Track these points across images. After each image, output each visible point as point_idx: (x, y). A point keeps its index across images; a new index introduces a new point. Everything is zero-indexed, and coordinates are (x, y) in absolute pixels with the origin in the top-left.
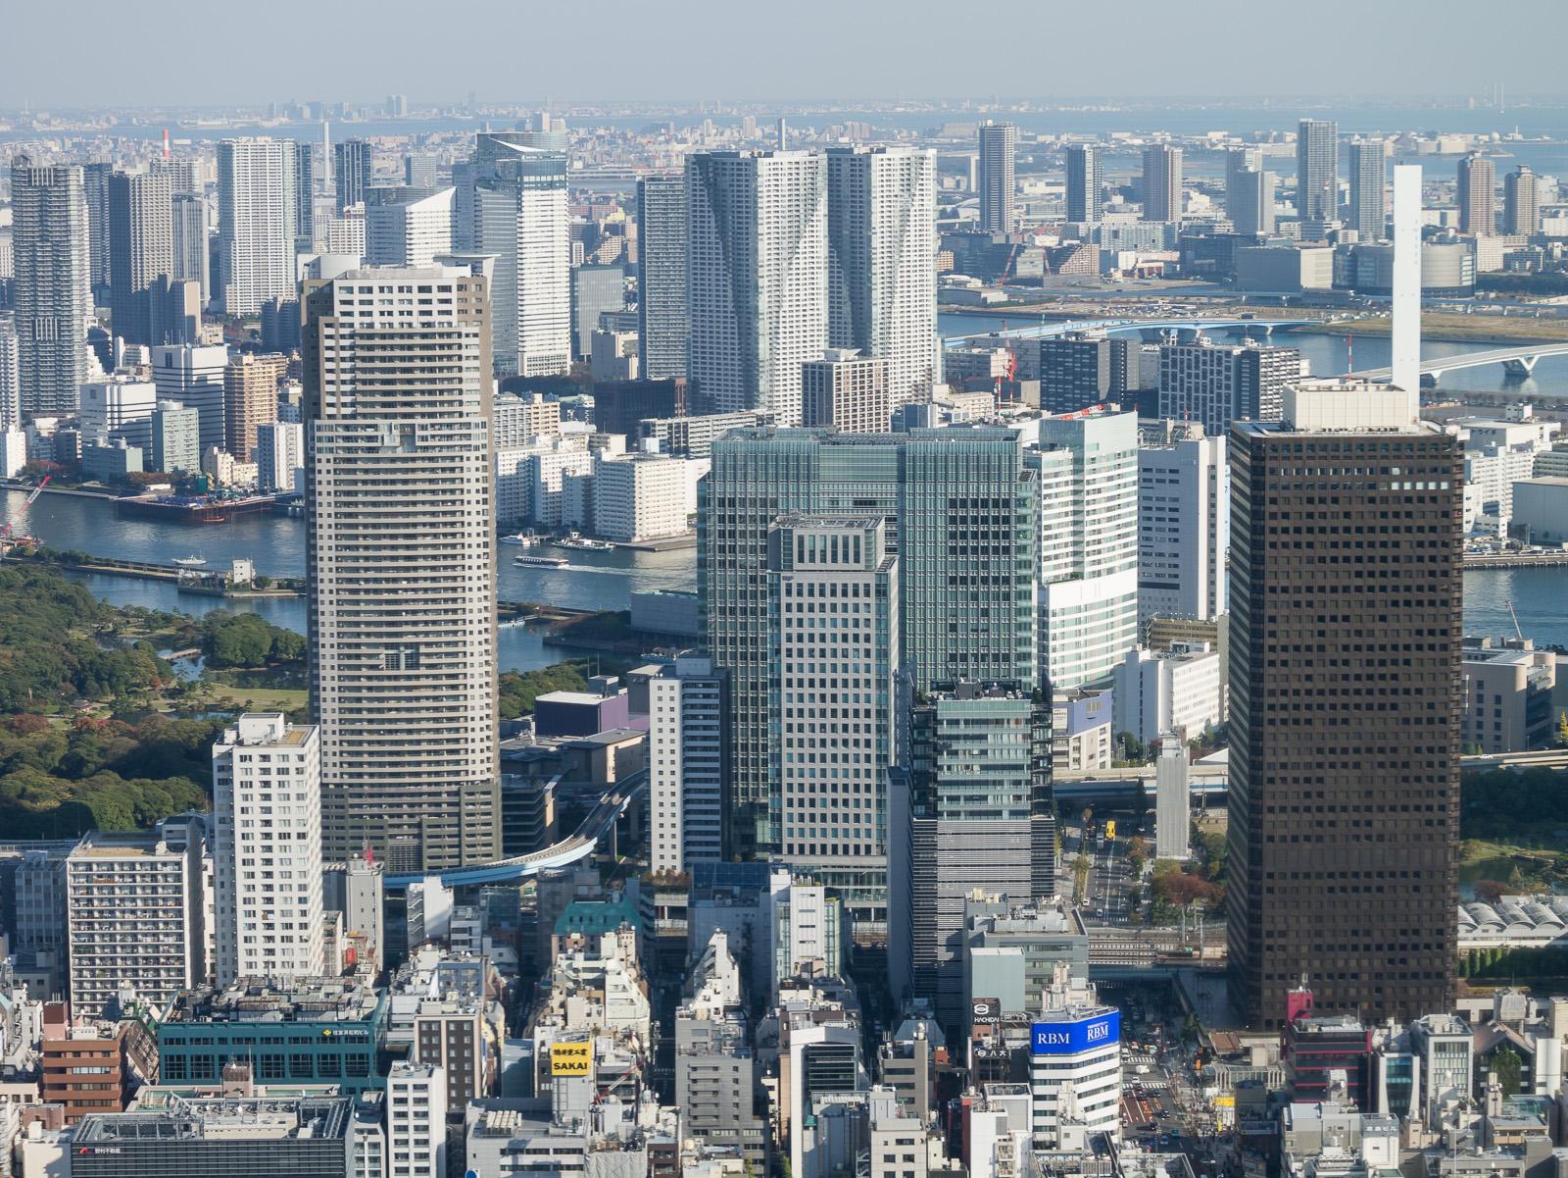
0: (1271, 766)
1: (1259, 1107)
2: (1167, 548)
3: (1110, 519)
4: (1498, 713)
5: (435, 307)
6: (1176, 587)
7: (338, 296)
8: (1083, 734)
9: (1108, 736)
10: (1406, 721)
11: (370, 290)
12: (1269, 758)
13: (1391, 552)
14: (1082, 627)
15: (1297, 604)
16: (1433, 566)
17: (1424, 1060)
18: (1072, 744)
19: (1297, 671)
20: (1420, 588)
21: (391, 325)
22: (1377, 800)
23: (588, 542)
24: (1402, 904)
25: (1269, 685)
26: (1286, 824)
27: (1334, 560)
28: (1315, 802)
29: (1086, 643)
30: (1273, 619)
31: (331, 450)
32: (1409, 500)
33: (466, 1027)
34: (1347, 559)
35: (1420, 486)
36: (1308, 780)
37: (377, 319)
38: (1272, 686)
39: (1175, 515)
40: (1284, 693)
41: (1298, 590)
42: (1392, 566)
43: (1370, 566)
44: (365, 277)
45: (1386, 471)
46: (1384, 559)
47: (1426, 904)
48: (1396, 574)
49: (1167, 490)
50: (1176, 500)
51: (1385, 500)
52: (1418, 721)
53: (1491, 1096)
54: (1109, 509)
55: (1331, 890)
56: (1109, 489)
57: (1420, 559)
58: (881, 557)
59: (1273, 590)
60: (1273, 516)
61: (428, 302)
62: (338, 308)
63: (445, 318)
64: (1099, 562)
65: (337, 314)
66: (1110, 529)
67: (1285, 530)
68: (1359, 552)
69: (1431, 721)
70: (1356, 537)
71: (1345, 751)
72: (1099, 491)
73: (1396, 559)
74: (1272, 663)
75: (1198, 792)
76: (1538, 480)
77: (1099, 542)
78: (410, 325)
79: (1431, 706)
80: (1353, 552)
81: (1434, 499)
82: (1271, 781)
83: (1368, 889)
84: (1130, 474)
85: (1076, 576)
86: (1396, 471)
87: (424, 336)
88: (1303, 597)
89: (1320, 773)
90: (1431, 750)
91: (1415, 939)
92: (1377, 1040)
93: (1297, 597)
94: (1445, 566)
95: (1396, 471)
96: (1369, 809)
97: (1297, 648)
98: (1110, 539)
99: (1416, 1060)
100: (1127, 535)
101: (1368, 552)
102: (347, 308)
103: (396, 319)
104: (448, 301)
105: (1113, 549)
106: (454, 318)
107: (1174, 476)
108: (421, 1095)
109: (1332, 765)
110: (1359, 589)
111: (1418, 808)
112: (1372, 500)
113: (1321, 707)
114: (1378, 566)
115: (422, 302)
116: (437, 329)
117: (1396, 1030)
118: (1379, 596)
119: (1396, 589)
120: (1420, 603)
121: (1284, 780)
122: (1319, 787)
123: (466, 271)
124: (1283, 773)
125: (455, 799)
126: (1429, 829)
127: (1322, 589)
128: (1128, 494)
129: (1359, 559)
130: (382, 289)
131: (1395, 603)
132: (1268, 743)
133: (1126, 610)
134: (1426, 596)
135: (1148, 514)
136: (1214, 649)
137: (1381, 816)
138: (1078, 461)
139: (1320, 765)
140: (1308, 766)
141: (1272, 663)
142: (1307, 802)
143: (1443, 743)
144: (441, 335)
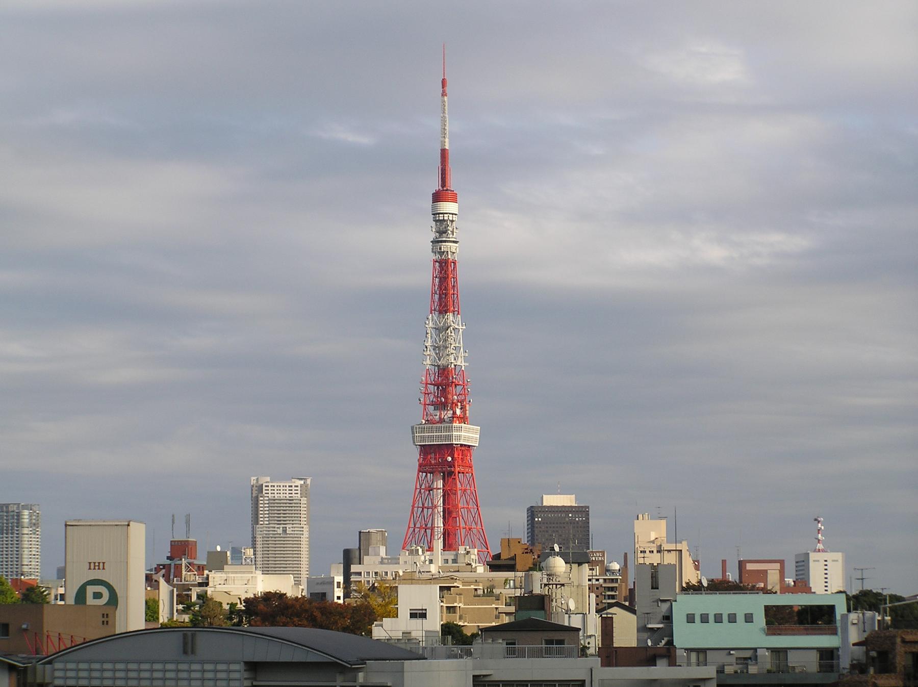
5: (293, 492)
7: (264, 488)
21: (280, 497)
37: (276, 496)
44: (272, 482)
65: (264, 493)
102: (267, 492)
104: (297, 490)
115: (289, 490)
123: (302, 482)
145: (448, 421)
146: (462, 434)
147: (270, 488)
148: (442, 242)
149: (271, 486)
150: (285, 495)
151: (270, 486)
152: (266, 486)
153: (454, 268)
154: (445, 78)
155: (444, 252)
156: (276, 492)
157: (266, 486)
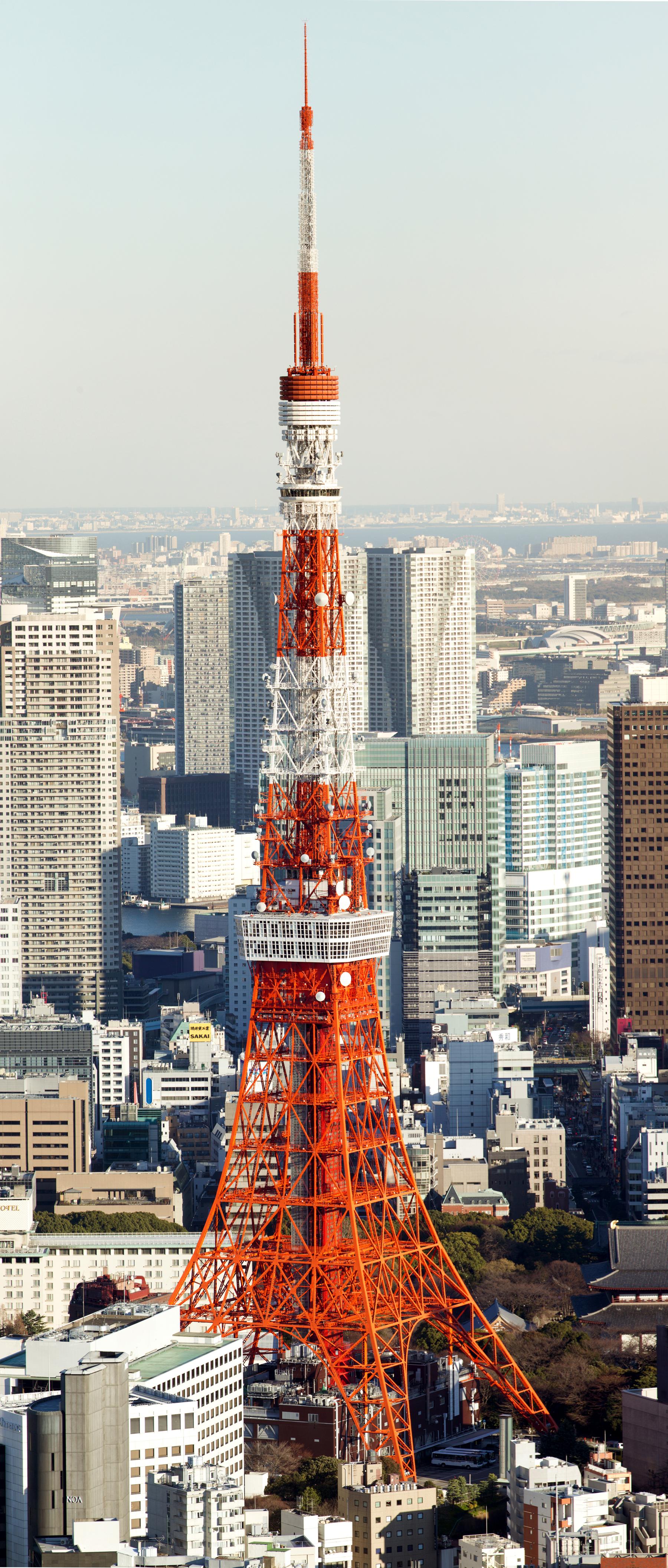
5: (81, 640)
7: (14, 633)
8: (549, 973)
9: (569, 977)
11: (37, 628)
18: (540, 980)
21: (51, 652)
23: (145, 903)
31: (9, 739)
33: (135, 1034)
37: (41, 648)
44: (32, 619)
58: (389, 814)
61: (77, 636)
62: (14, 641)
63: (88, 648)
78: (64, 652)
87: (73, 660)
103: (54, 648)
106: (94, 648)
108: (118, 1047)
116: (82, 655)
125: (93, 982)
130: (44, 628)
132: (626, 901)
144: (85, 659)
145: (318, 906)
146: (350, 940)
147: (27, 633)
148: (303, 493)
149: (30, 628)
150: (61, 648)
151: (27, 628)
152: (19, 628)
153: (331, 548)
154: (309, 105)
155: (307, 517)
156: (41, 641)
157: (19, 628)
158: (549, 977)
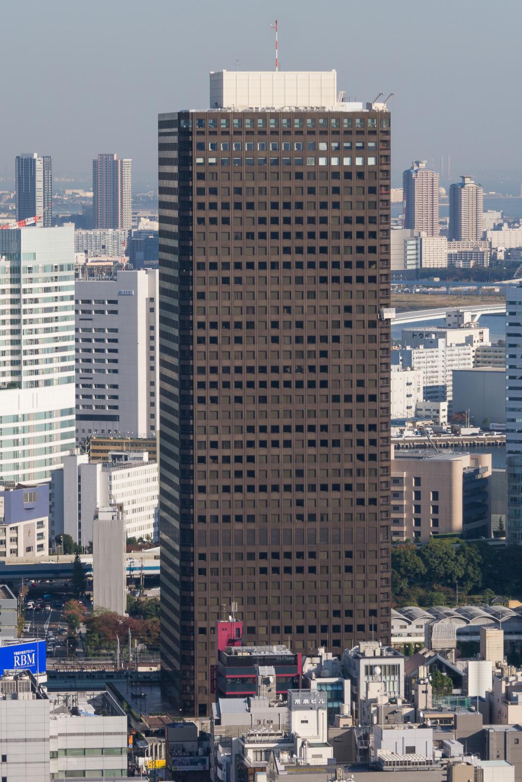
0: (202, 445)
1: (190, 746)
2: (107, 379)
3: (47, 330)
4: (436, 509)
6: (114, 418)
8: (21, 525)
9: (46, 530)
10: (336, 399)
12: (199, 437)
13: (318, 228)
14: (20, 436)
15: (226, 281)
16: (360, 242)
17: (355, 683)
18: (10, 534)
19: (227, 348)
20: (348, 265)
22: (306, 481)
24: (334, 585)
25: (197, 363)
26: (217, 504)
27: (263, 236)
28: (245, 481)
29: (24, 453)
30: (201, 296)
32: (336, 175)
34: (275, 235)
35: (347, 161)
36: (238, 459)
38: (202, 363)
39: (114, 346)
40: (214, 370)
41: (226, 266)
42: (320, 243)
43: (298, 243)
45: (315, 146)
46: (311, 235)
47: (359, 585)
48: (324, 250)
49: (107, 321)
50: (116, 330)
51: (312, 175)
52: (348, 399)
53: (421, 688)
54: (46, 320)
55: (263, 571)
56: (46, 300)
57: (348, 235)
59: (201, 266)
60: (201, 191)
64: (36, 372)
66: (48, 340)
67: (213, 206)
68: (287, 228)
69: (360, 398)
70: (282, 213)
71: (275, 429)
72: (36, 301)
73: (324, 235)
74: (201, 340)
75: (136, 574)
76: (476, 369)
77: (36, 352)
79: (361, 383)
80: (281, 228)
81: (360, 175)
82: (202, 460)
83: (300, 570)
84: (67, 288)
85: (13, 385)
86: (323, 146)
88: (232, 273)
89: (251, 452)
90: (361, 428)
91: (348, 621)
92: (308, 666)
93: (226, 273)
94: (372, 242)
95: (323, 146)
96: (300, 488)
97: (226, 325)
98: (47, 351)
99: (347, 683)
100: (65, 349)
101: (294, 228)
105: (51, 361)
107: (113, 307)
109: (263, 444)
110: (287, 265)
111: (349, 487)
112: (299, 176)
113: (251, 384)
114: (306, 243)
117: (325, 655)
118: (307, 273)
119: (324, 265)
120: (348, 280)
121: (215, 459)
122: (250, 466)
124: (214, 452)
126: (361, 509)
127: (250, 265)
128: (66, 308)
129: (287, 235)
131: (324, 280)
132: (198, 422)
133: (64, 424)
134: (354, 273)
135: (87, 391)
136: (152, 459)
137: (312, 495)
138: (16, 270)
139: (251, 444)
140: (239, 444)
141: (202, 400)
142: (239, 482)
143: (373, 421)
158: (21, 530)
